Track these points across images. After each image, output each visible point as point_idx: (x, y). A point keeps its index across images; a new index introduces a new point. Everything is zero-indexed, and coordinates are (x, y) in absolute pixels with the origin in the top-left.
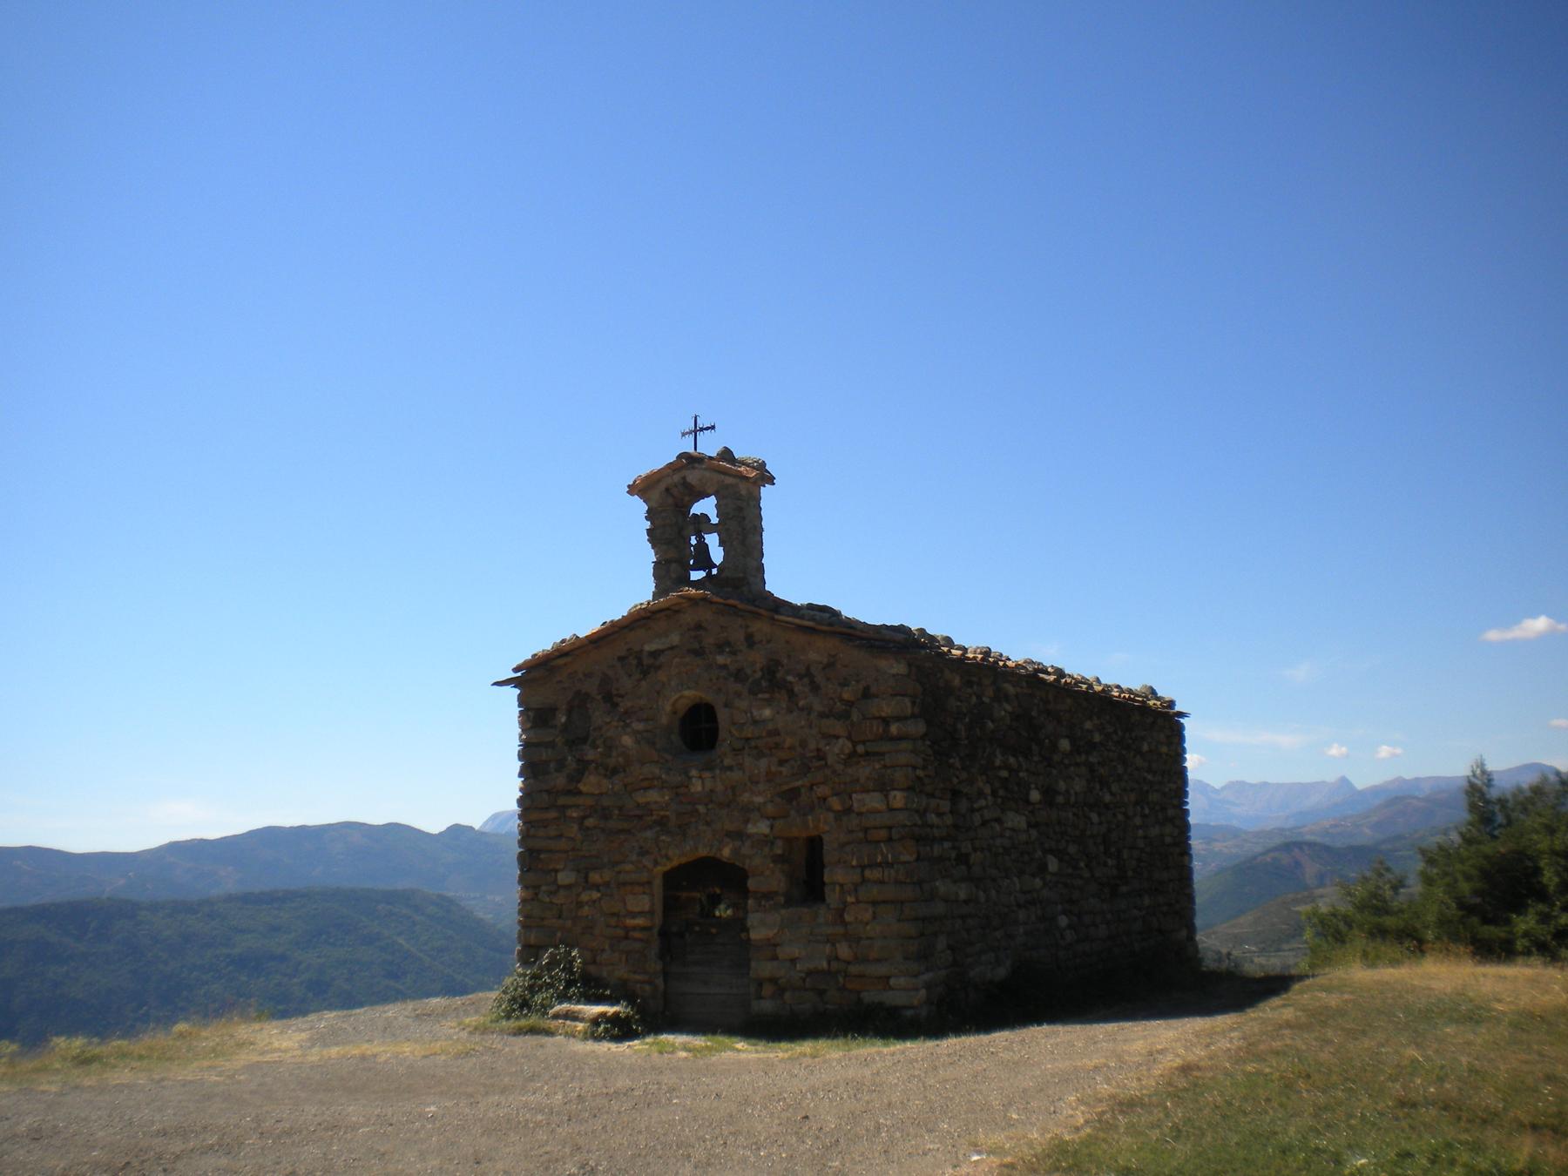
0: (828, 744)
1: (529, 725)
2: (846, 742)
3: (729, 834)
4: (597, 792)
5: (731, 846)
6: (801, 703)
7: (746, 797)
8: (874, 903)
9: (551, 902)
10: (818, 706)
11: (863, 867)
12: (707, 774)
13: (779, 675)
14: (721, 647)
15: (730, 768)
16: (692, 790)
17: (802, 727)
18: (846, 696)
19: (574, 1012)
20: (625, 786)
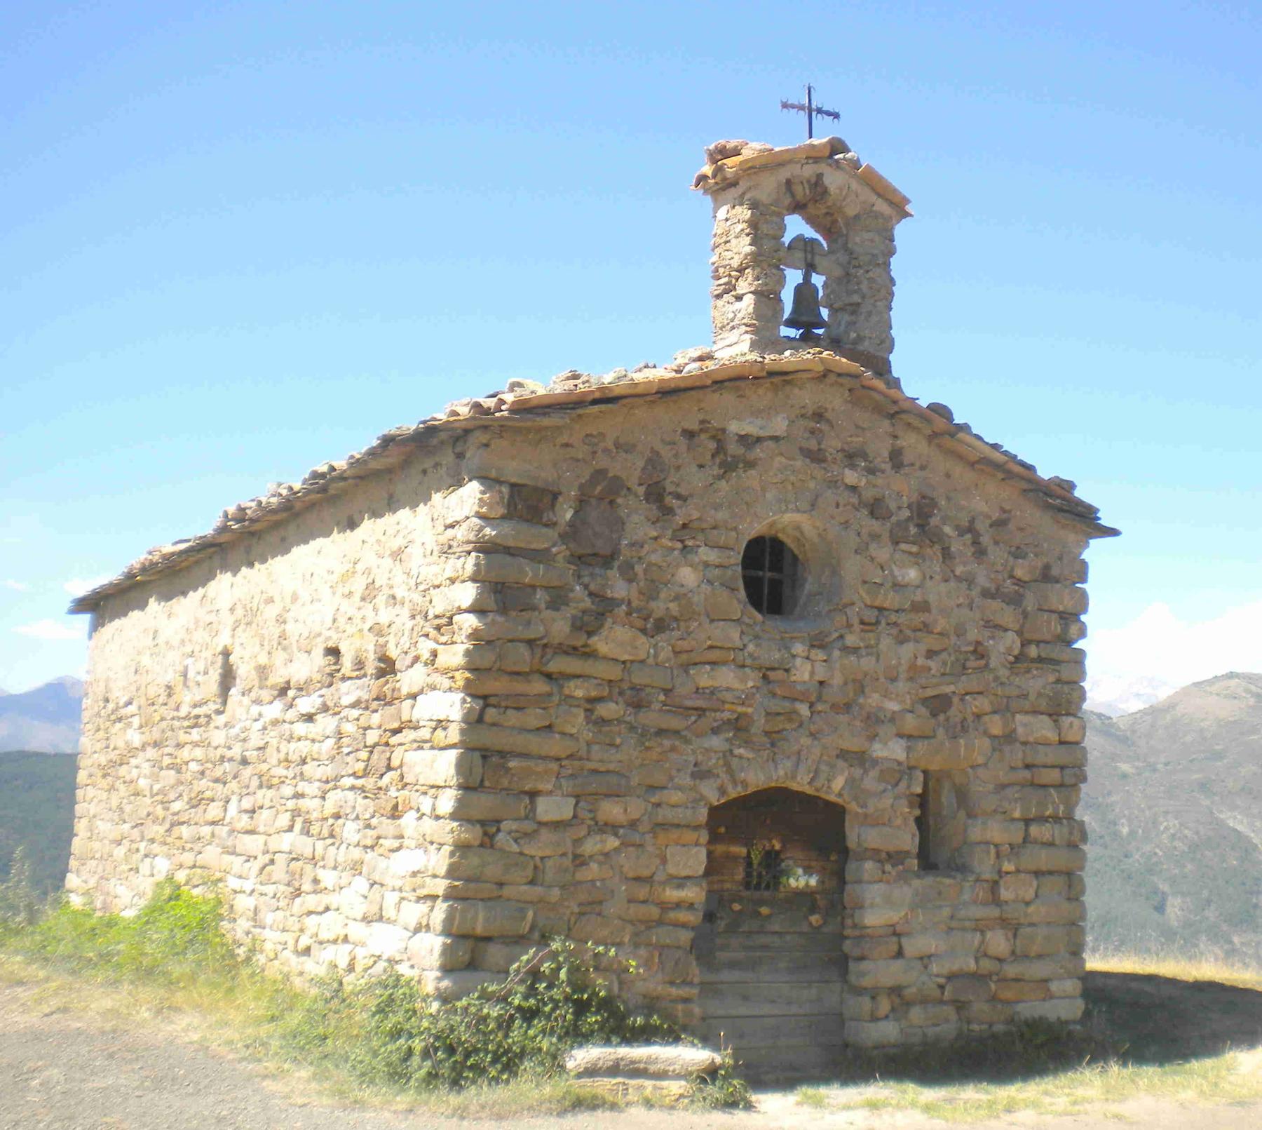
0: (993, 638)
1: (501, 511)
2: (1016, 637)
3: (843, 754)
4: (626, 657)
5: (846, 774)
6: (959, 570)
7: (873, 700)
8: (1037, 874)
9: (521, 854)
10: (982, 580)
11: (1028, 822)
12: (819, 655)
13: (934, 521)
14: (851, 457)
15: (855, 650)
17: (959, 606)
18: (1019, 573)
19: (632, 1062)
20: (677, 653)
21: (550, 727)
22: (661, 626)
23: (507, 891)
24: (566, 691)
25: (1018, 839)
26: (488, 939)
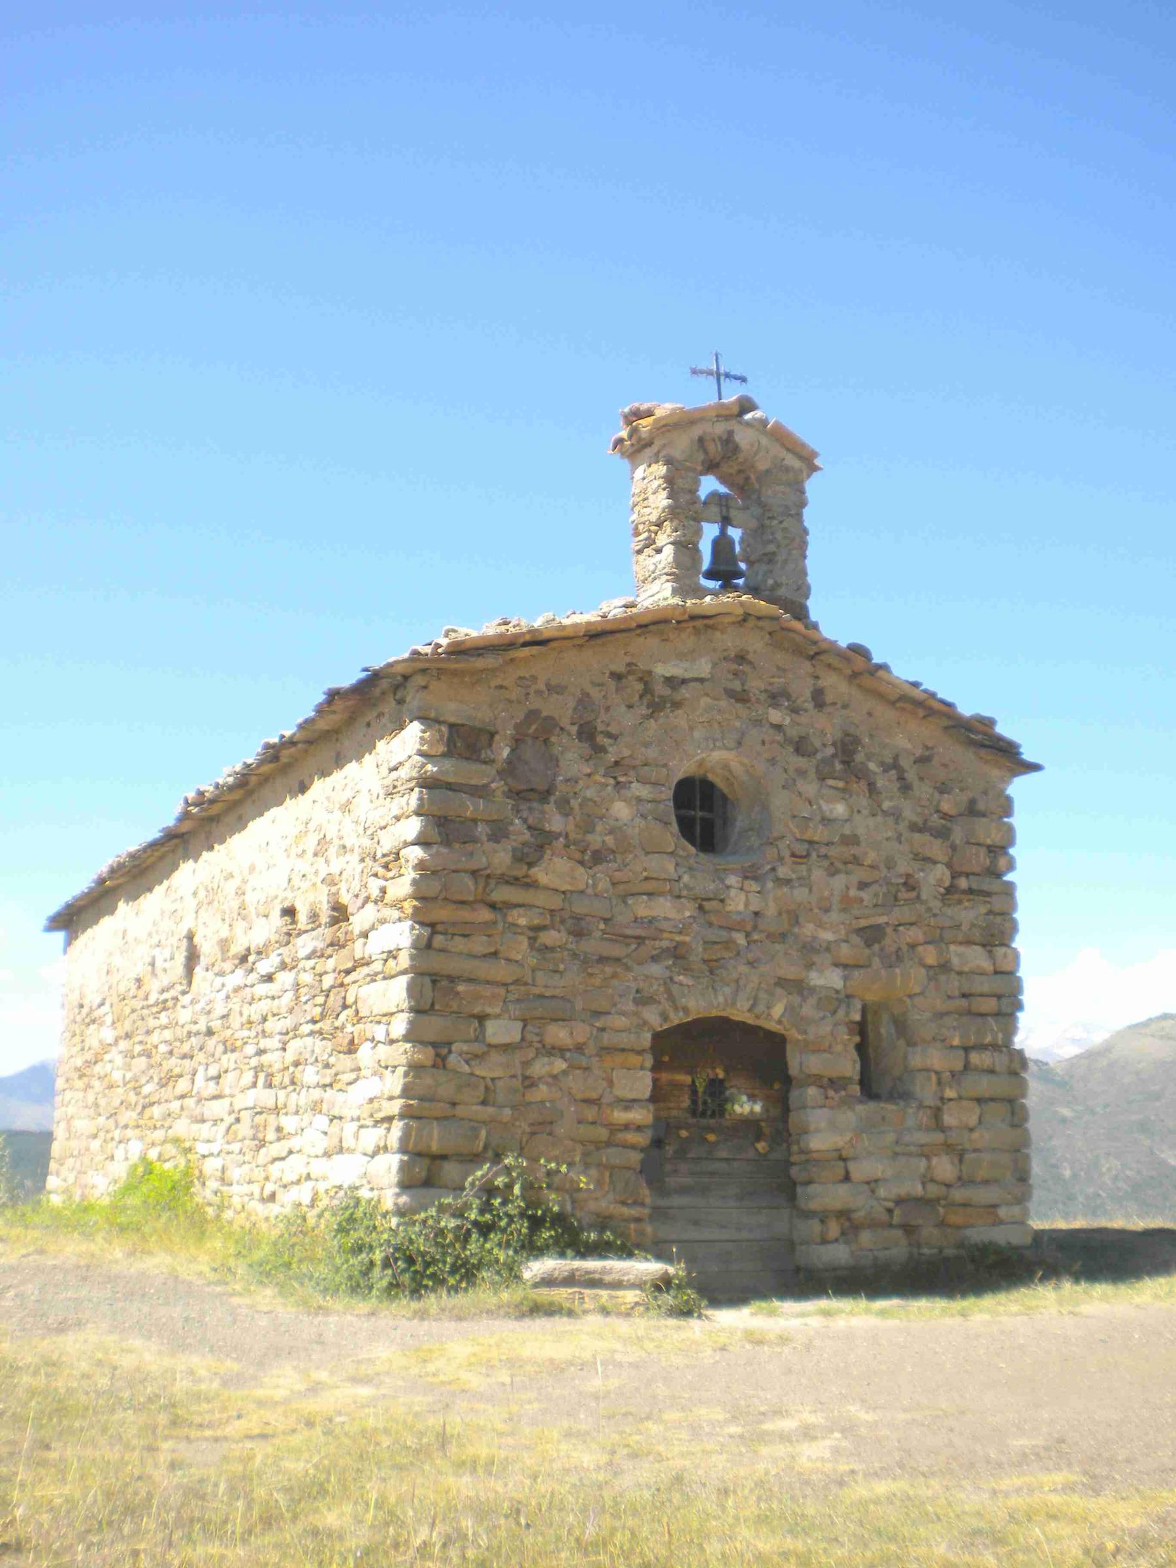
0: (922, 870)
1: (442, 749)
3: (781, 982)
5: (785, 1001)
6: (886, 805)
8: (979, 1100)
9: (472, 1074)
10: (909, 814)
11: (967, 1049)
12: (754, 886)
13: (859, 757)
14: (775, 698)
15: (788, 882)
16: (729, 908)
17: (887, 839)
18: (946, 807)
19: (588, 1272)
21: (495, 954)
22: (598, 857)
23: (460, 1111)
24: (510, 919)
25: (959, 1066)
26: (444, 1157)
